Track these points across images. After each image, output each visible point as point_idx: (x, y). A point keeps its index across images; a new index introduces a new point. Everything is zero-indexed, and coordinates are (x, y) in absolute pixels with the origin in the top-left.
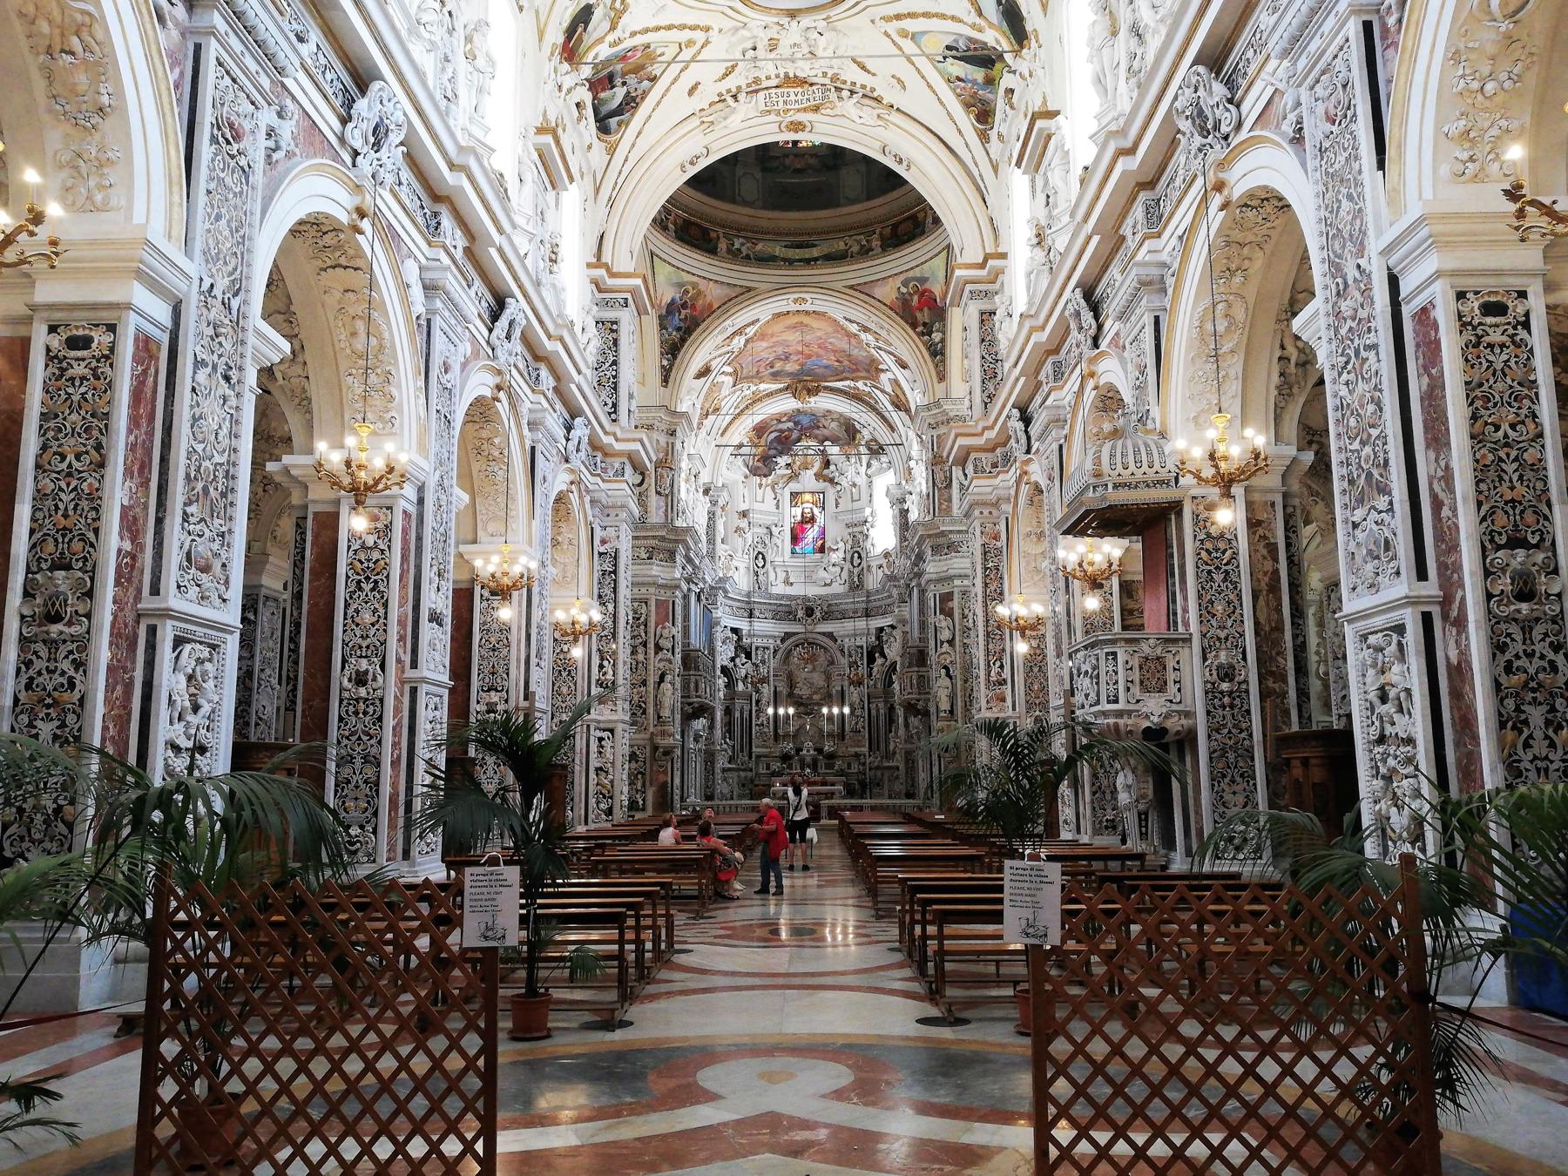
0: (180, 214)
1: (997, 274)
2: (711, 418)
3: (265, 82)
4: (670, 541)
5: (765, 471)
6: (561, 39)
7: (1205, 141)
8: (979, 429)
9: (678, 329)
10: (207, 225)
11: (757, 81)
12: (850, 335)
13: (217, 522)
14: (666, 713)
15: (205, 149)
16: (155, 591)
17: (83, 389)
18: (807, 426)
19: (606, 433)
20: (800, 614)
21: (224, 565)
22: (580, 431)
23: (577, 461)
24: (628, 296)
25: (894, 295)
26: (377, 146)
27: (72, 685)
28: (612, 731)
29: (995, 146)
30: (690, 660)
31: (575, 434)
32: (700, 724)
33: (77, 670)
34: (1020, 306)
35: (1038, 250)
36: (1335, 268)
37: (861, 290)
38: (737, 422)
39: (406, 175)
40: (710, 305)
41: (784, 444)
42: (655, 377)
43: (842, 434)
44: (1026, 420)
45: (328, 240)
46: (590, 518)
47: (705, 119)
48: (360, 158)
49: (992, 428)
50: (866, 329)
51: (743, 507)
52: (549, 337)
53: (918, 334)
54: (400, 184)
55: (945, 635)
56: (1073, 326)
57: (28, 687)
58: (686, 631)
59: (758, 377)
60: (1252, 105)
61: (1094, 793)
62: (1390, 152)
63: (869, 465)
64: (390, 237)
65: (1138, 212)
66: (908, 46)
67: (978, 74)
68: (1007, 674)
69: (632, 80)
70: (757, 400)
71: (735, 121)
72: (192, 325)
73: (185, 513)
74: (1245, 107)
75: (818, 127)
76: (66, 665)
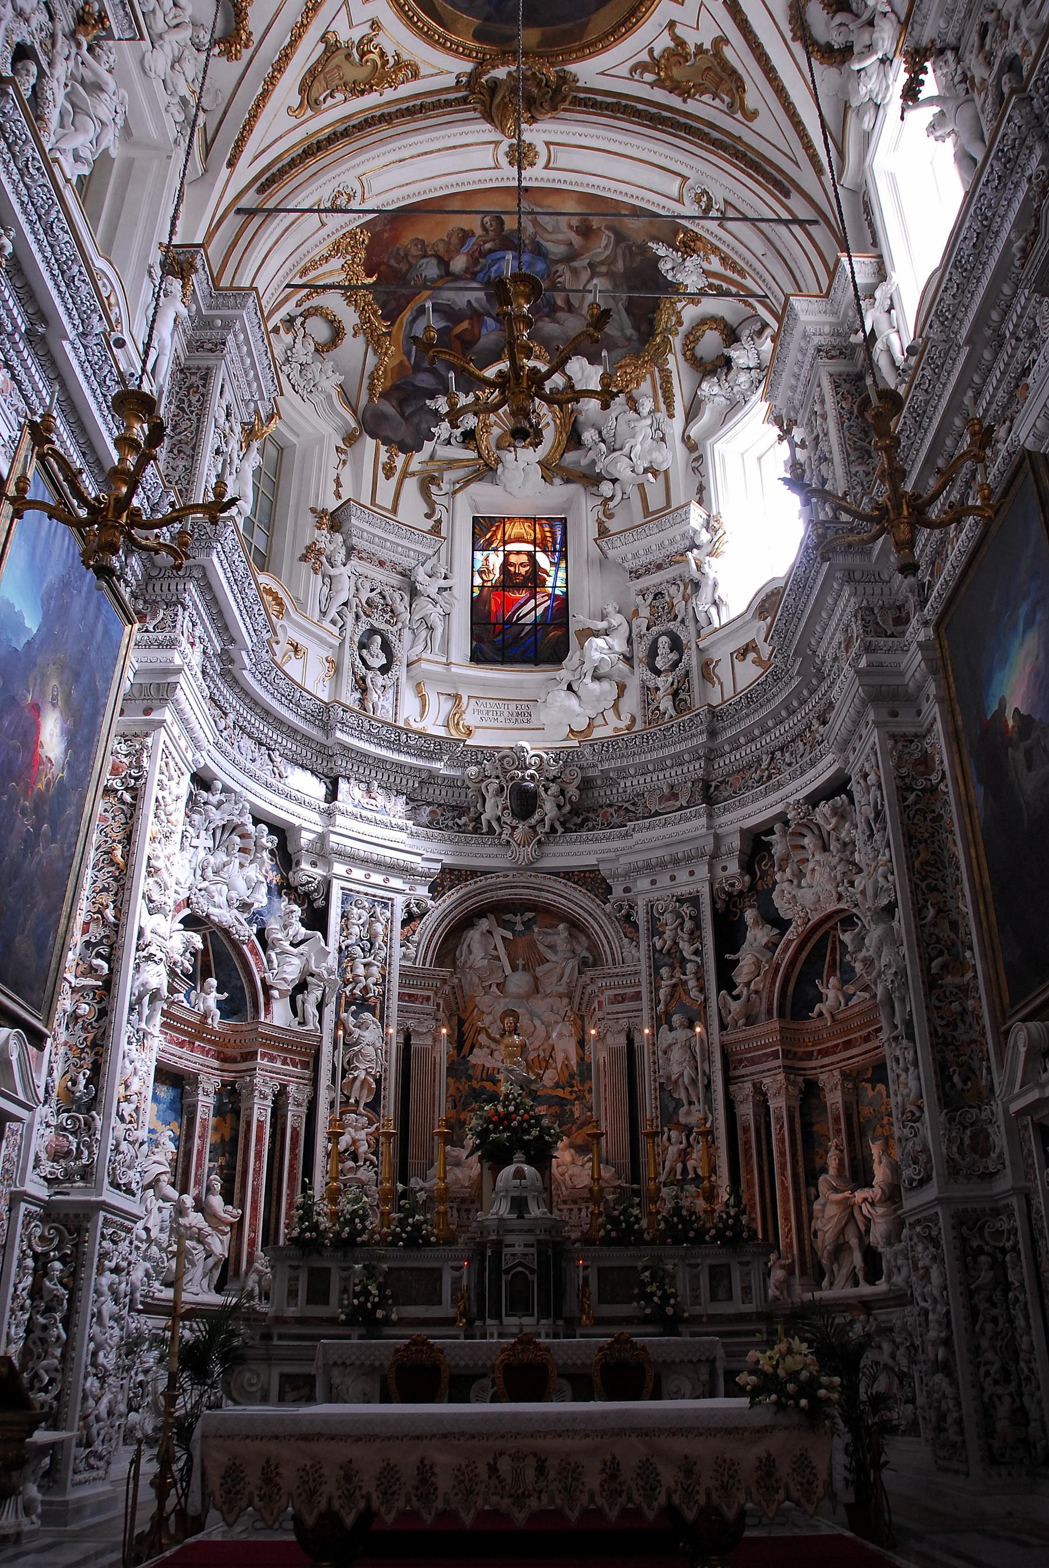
5: (403, 431)
43: (620, 326)
51: (332, 504)
63: (692, 413)
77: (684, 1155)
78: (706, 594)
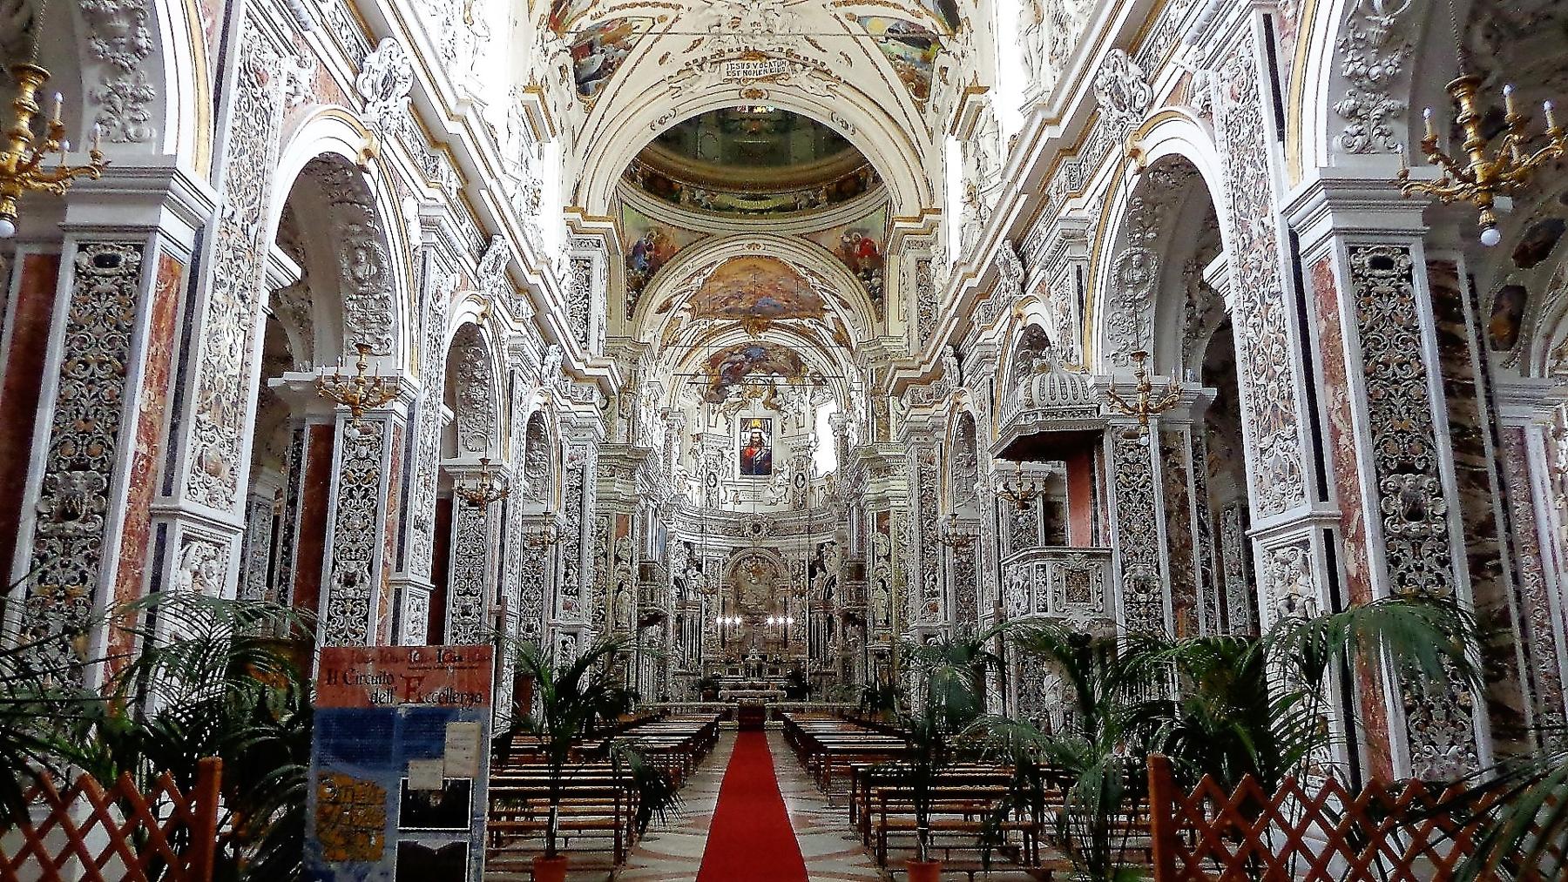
0: (206, 151)
1: (933, 226)
2: (671, 349)
3: (288, 33)
4: (632, 460)
6: (548, 10)
7: (1122, 114)
8: (917, 362)
10: (231, 159)
11: (721, 52)
12: (798, 277)
13: (227, 429)
14: (624, 621)
15: (233, 92)
16: (167, 491)
17: (108, 304)
18: (757, 358)
19: (577, 360)
20: (748, 530)
21: (232, 469)
22: (553, 357)
23: (548, 386)
24: (601, 237)
26: (385, 95)
27: (84, 579)
28: (575, 635)
29: (930, 117)
30: (645, 572)
31: (550, 359)
32: (654, 630)
33: (89, 565)
34: (955, 255)
35: (969, 207)
36: (1241, 224)
37: (811, 238)
38: (694, 354)
39: (408, 122)
41: (736, 374)
42: (622, 310)
44: (960, 358)
45: (338, 177)
46: (560, 437)
47: (674, 85)
48: (369, 106)
49: (927, 363)
50: (813, 273)
51: (698, 431)
52: (531, 271)
53: (859, 278)
54: (404, 130)
55: (883, 550)
56: (1002, 272)
57: (41, 580)
58: (643, 541)
59: (714, 313)
60: (1164, 83)
61: (1020, 696)
62: (1291, 126)
64: (390, 175)
65: (1062, 176)
66: (855, 28)
67: (917, 53)
68: (939, 587)
69: (610, 48)
70: (712, 333)
71: (700, 87)
72: (213, 248)
73: (198, 420)
74: (1157, 87)
75: (774, 95)
76: (79, 560)
77: (798, 632)
78: (813, 464)
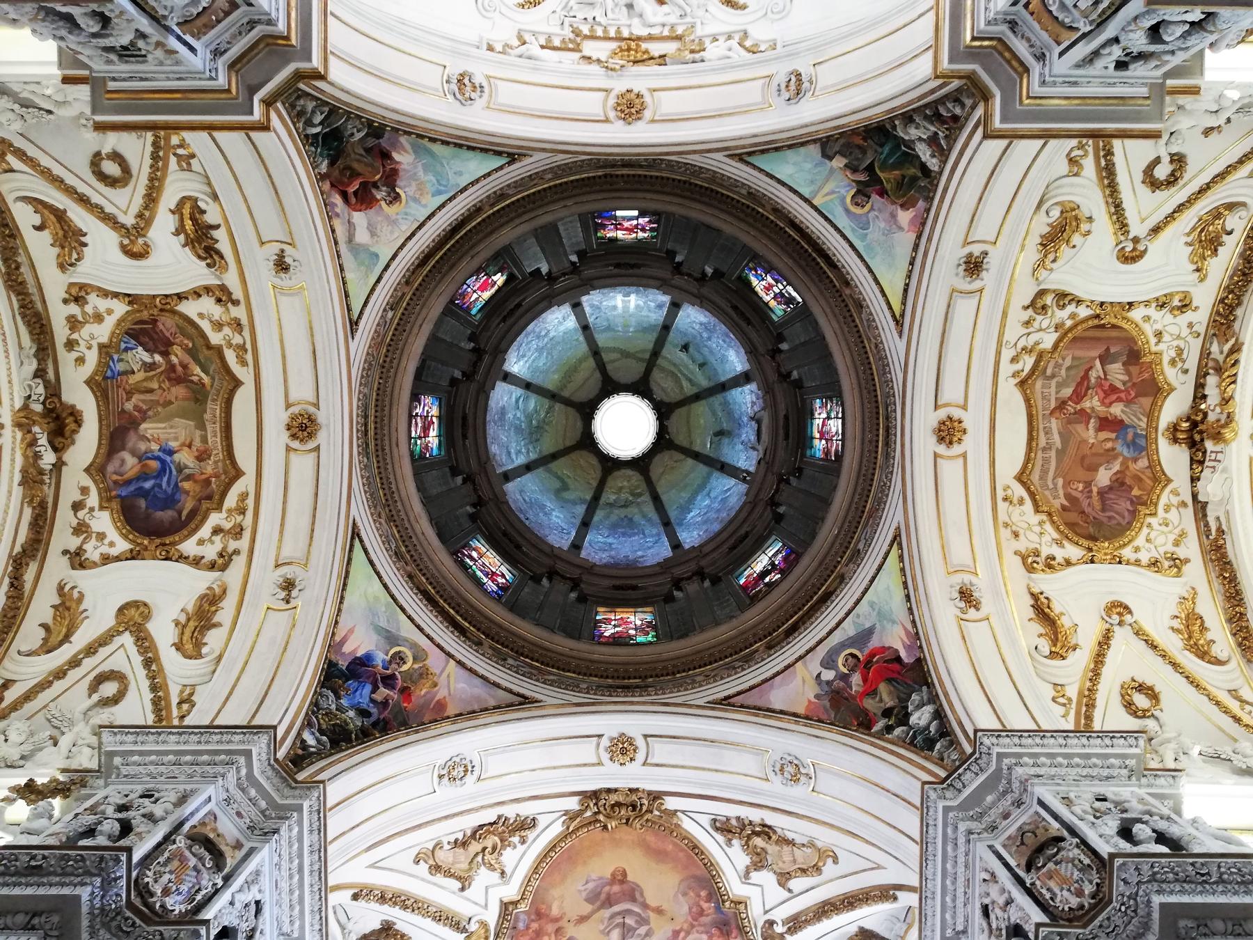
9: (363, 713)
25: (811, 691)
40: (441, 705)
